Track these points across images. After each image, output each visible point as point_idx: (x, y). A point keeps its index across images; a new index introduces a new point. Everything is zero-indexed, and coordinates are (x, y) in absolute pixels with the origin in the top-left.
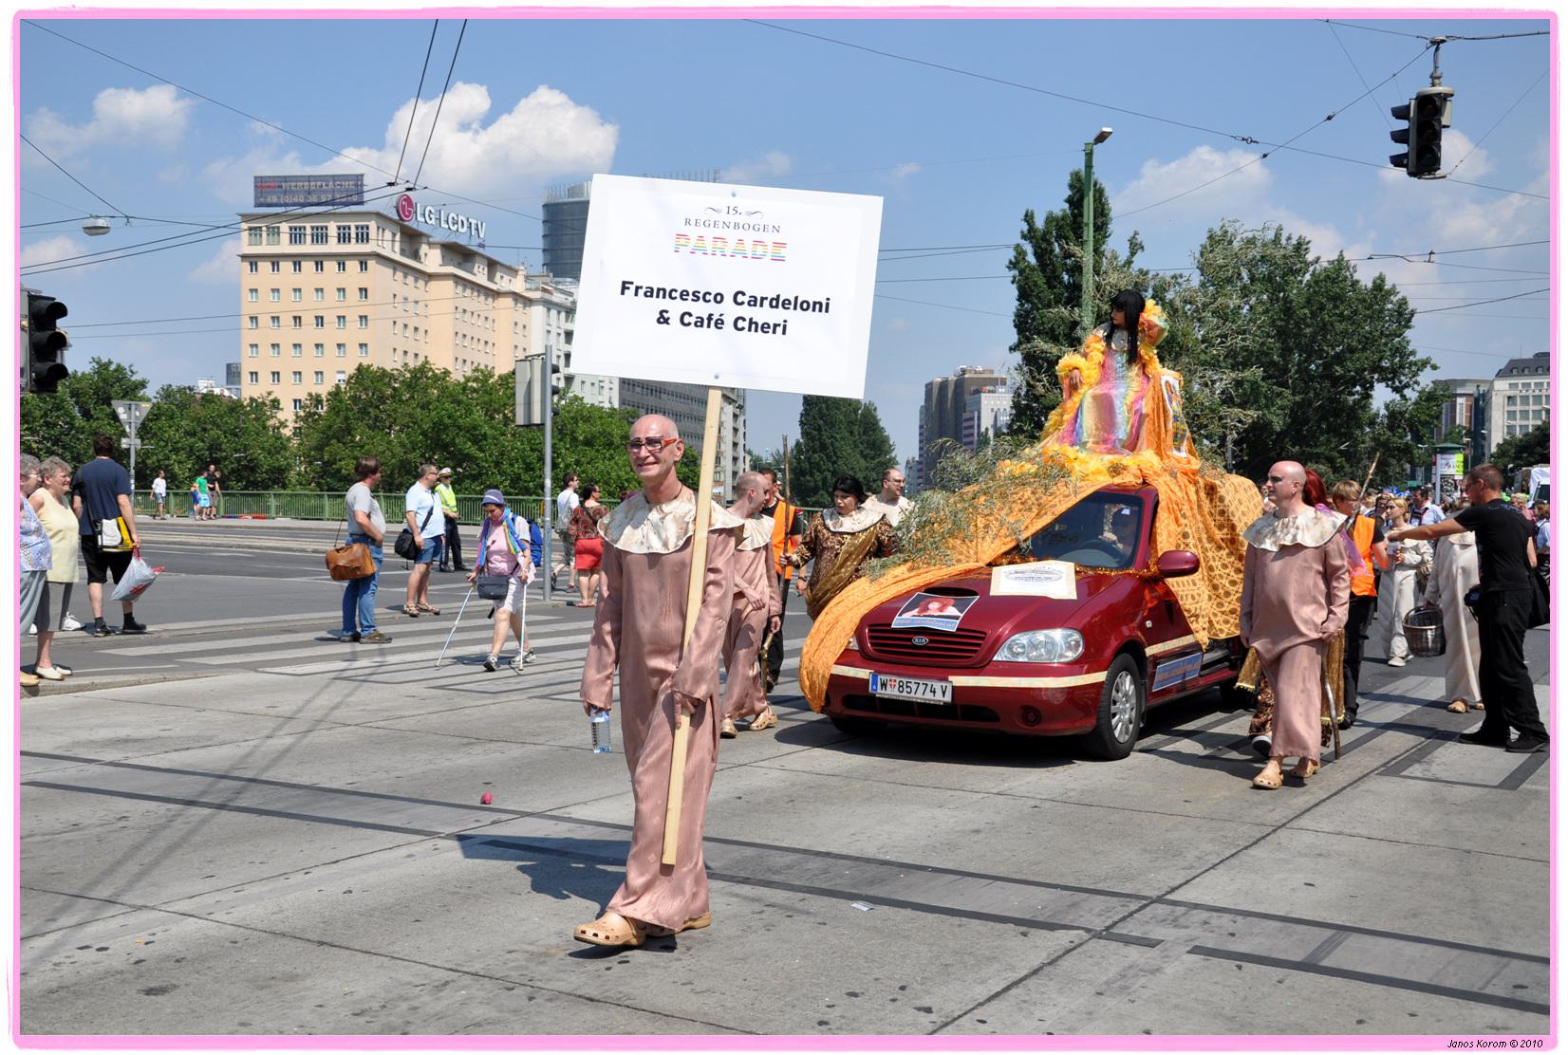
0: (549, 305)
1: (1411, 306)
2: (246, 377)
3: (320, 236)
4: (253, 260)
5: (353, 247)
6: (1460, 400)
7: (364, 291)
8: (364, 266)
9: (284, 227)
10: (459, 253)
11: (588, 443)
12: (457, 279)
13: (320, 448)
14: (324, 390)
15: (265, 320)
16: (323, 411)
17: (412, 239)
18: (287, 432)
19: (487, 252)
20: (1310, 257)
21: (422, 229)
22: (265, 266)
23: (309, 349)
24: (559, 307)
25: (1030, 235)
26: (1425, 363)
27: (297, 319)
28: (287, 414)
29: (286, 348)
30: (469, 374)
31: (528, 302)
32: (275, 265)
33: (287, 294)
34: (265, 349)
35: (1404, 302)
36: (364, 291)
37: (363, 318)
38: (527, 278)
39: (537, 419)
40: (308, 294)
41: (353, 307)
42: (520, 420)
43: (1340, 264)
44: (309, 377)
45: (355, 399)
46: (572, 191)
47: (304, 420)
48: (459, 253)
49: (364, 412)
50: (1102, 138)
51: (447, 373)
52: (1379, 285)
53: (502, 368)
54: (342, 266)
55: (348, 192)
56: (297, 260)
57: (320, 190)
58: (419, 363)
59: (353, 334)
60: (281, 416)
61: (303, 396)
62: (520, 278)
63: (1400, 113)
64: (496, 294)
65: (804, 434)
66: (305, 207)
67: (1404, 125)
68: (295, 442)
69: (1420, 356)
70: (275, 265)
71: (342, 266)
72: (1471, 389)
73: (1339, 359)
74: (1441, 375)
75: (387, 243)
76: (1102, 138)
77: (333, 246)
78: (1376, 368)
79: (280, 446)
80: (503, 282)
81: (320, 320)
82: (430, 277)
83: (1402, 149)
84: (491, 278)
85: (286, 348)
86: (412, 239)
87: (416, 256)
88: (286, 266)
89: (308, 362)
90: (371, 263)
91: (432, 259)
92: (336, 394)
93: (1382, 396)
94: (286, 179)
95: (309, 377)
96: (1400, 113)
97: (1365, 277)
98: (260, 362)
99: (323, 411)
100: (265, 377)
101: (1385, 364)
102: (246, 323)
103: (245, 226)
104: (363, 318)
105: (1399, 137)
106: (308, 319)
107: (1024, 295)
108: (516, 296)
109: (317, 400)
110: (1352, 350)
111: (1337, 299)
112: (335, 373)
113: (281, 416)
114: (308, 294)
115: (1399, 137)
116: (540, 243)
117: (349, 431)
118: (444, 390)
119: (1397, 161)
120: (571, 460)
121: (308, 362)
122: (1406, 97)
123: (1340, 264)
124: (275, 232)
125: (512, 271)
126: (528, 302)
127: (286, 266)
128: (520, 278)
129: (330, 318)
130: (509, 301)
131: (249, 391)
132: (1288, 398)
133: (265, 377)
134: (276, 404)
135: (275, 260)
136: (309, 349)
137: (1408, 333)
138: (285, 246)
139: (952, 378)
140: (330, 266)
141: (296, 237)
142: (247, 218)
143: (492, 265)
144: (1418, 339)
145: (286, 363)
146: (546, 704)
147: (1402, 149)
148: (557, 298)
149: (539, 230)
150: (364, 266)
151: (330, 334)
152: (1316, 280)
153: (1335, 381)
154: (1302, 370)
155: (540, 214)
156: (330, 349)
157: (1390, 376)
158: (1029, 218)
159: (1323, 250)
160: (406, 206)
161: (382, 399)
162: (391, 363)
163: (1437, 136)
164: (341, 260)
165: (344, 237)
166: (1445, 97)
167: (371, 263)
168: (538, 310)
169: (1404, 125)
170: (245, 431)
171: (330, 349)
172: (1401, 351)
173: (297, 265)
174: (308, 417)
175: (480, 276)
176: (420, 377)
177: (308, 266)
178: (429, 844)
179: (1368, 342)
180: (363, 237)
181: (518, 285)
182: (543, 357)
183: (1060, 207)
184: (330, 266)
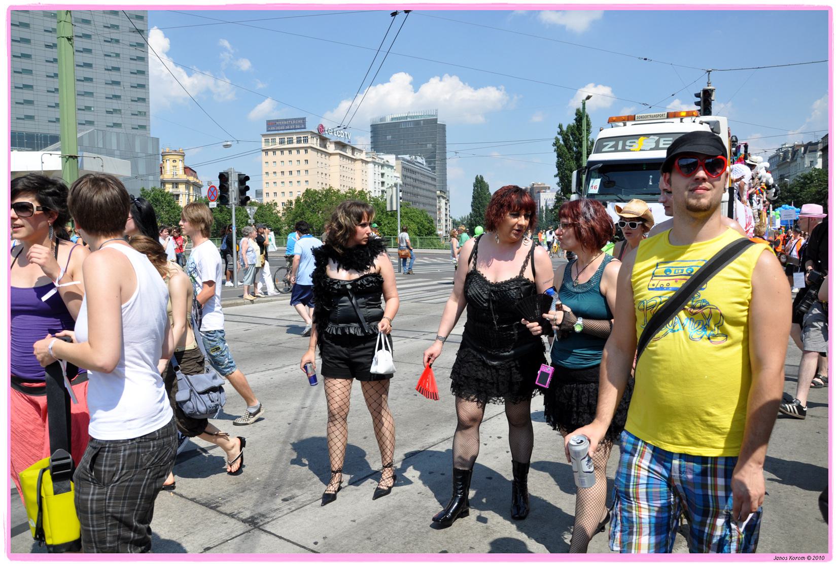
0: (375, 163)
2: (264, 195)
3: (290, 141)
4: (266, 151)
5: (302, 145)
7: (306, 161)
8: (306, 151)
9: (278, 140)
10: (341, 145)
11: (392, 216)
12: (341, 155)
13: (293, 220)
14: (293, 199)
15: (271, 175)
16: (293, 206)
17: (324, 140)
18: (280, 215)
19: (352, 144)
21: (327, 136)
22: (270, 153)
23: (287, 183)
24: (379, 164)
25: (561, 133)
27: (283, 172)
28: (280, 208)
29: (279, 183)
30: (347, 190)
31: (367, 162)
32: (274, 153)
33: (278, 163)
34: (271, 184)
36: (306, 161)
37: (307, 171)
38: (367, 153)
39: (394, 209)
40: (287, 163)
41: (303, 166)
42: (388, 209)
44: (287, 194)
45: (306, 202)
46: (381, 119)
47: (286, 210)
48: (341, 145)
49: (309, 206)
50: (588, 98)
51: (339, 191)
53: (358, 189)
54: (298, 152)
55: (302, 123)
56: (282, 150)
57: (290, 124)
58: (328, 187)
59: (303, 177)
60: (278, 209)
61: (285, 201)
62: (364, 153)
63: (697, 95)
64: (355, 160)
65: (473, 210)
66: (285, 130)
67: (699, 99)
68: (283, 218)
70: (274, 153)
71: (298, 152)
75: (314, 142)
77: (295, 145)
79: (278, 220)
80: (357, 156)
81: (291, 172)
82: (331, 154)
84: (353, 154)
85: (279, 183)
86: (324, 140)
87: (325, 147)
88: (278, 153)
89: (287, 188)
90: (309, 150)
91: (331, 148)
92: (298, 200)
94: (277, 121)
95: (287, 194)
96: (697, 95)
98: (270, 189)
99: (293, 206)
100: (271, 194)
102: (265, 176)
103: (263, 139)
104: (307, 171)
106: (287, 174)
107: (558, 156)
108: (363, 161)
109: (291, 203)
112: (298, 191)
113: (278, 209)
114: (287, 163)
115: (697, 104)
116: (369, 140)
117: (303, 214)
118: (338, 197)
120: (386, 222)
121: (287, 188)
122: (699, 90)
124: (274, 141)
125: (361, 151)
126: (367, 162)
127: (278, 153)
128: (364, 153)
129: (295, 173)
130: (359, 163)
131: (266, 200)
133: (271, 194)
134: (276, 204)
135: (274, 151)
136: (287, 183)
138: (278, 146)
139: (529, 187)
140: (294, 152)
141: (282, 142)
142: (263, 135)
143: (353, 149)
145: (279, 189)
146: (418, 304)
148: (377, 160)
149: (369, 135)
150: (306, 151)
151: (295, 178)
155: (369, 129)
156: (295, 183)
158: (560, 127)
160: (321, 128)
161: (315, 201)
162: (318, 188)
163: (710, 104)
164: (298, 149)
165: (299, 142)
166: (712, 90)
167: (309, 150)
168: (371, 165)
169: (699, 99)
170: (265, 215)
171: (295, 183)
173: (282, 152)
174: (288, 209)
175: (349, 153)
176: (329, 193)
177: (286, 152)
178: (408, 340)
180: (306, 141)
181: (363, 156)
182: (396, 185)
183: (569, 120)
184: (294, 152)
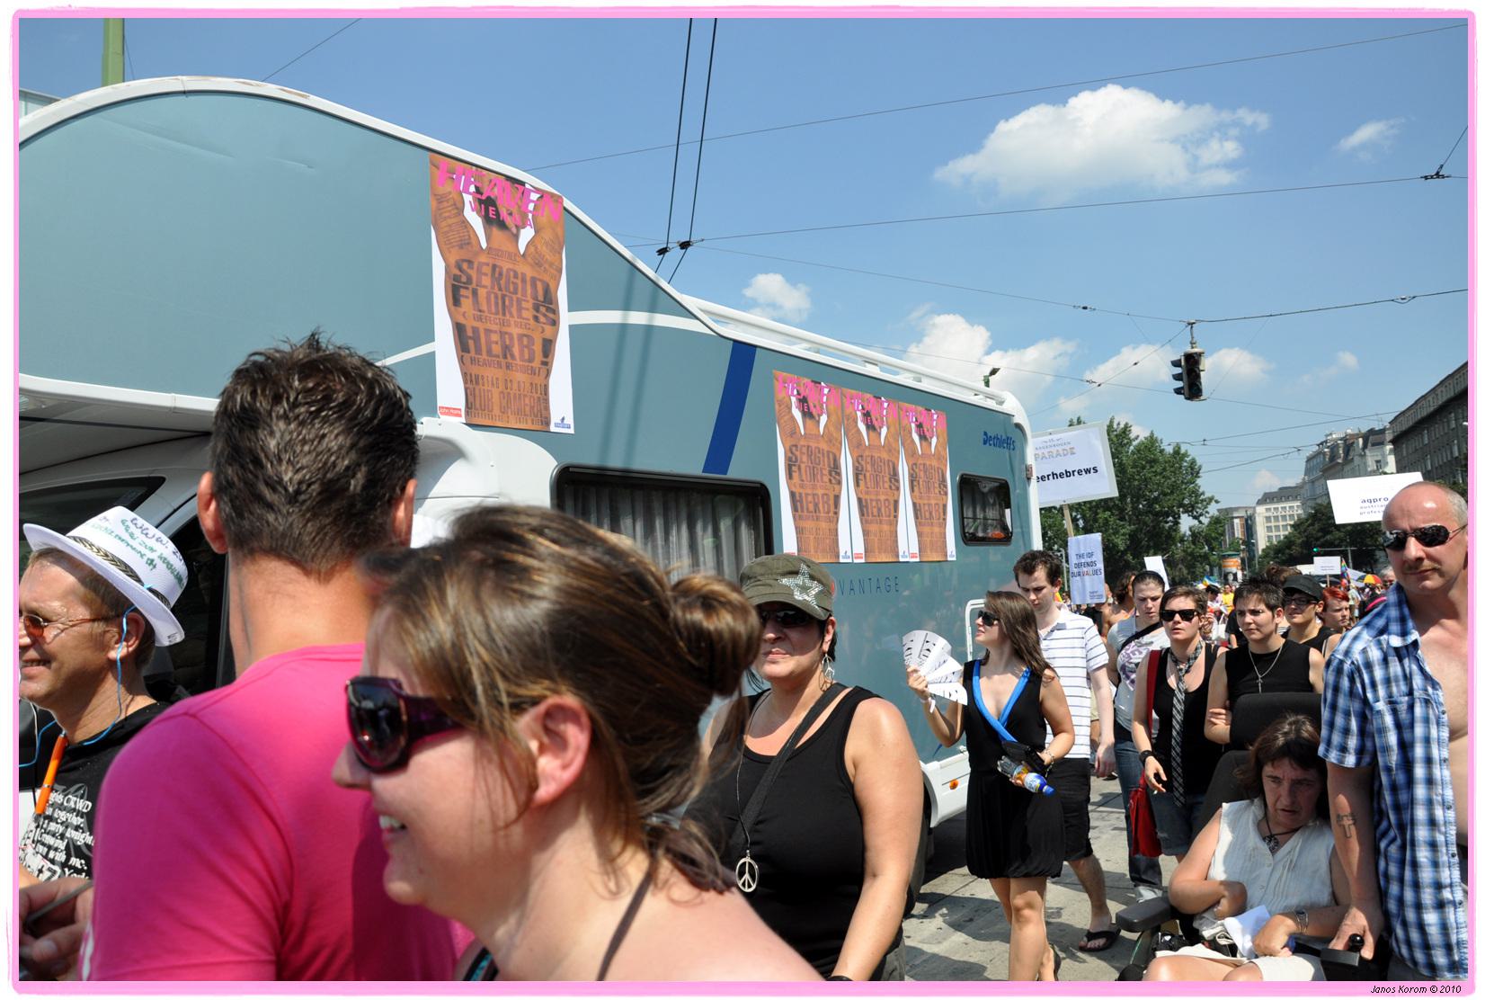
1: (1199, 462)
6: (1236, 521)
20: (1132, 436)
26: (1211, 499)
35: (1193, 462)
43: (1152, 441)
50: (994, 372)
52: (1177, 452)
63: (1176, 364)
67: (1179, 370)
69: (1208, 495)
72: (1242, 514)
73: (1156, 500)
74: (1222, 506)
76: (994, 372)
78: (1181, 505)
83: (1180, 384)
93: (1186, 523)
96: (1176, 364)
97: (1169, 450)
101: (1186, 502)
105: (1177, 377)
110: (1165, 494)
111: (1154, 462)
115: (1177, 377)
119: (1178, 391)
122: (1179, 355)
123: (1152, 441)
132: (1128, 529)
137: (1199, 481)
144: (1206, 484)
147: (1180, 384)
152: (1138, 449)
153: (1157, 514)
154: (1135, 508)
157: (1190, 510)
159: (1139, 433)
166: (1200, 355)
169: (1179, 370)
172: (1196, 493)
179: (1174, 488)
